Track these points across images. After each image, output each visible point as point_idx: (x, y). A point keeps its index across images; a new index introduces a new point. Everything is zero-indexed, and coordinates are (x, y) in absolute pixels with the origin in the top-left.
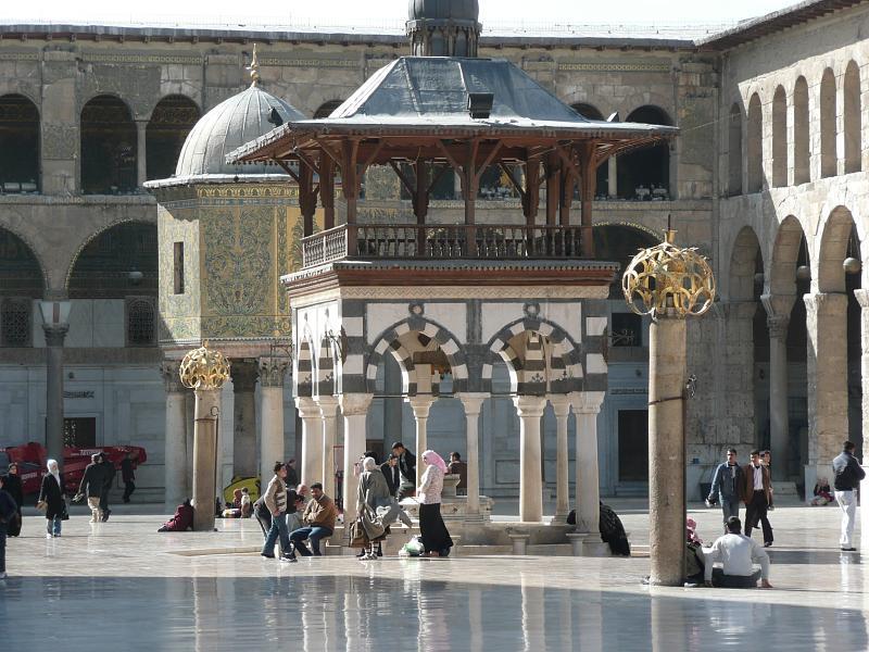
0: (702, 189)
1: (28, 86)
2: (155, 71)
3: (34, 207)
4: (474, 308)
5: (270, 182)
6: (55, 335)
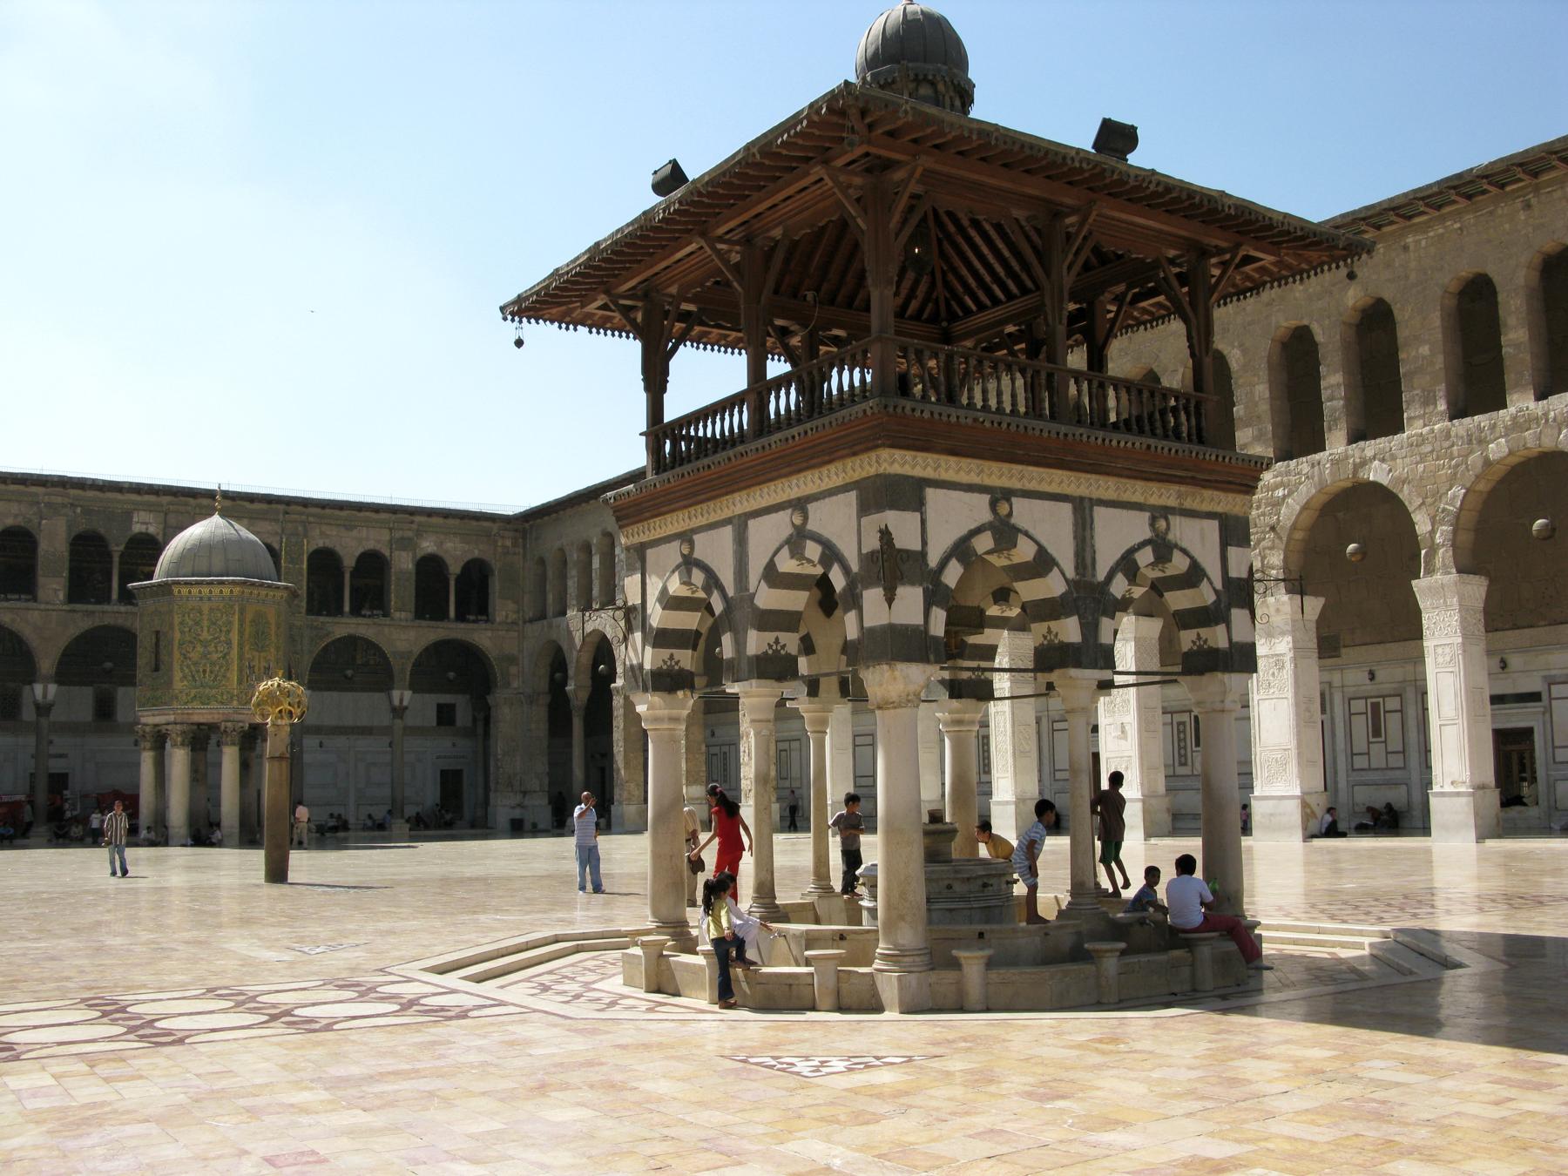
0: (512, 617)
2: (128, 516)
4: (1083, 510)
5: (233, 582)
6: (43, 709)
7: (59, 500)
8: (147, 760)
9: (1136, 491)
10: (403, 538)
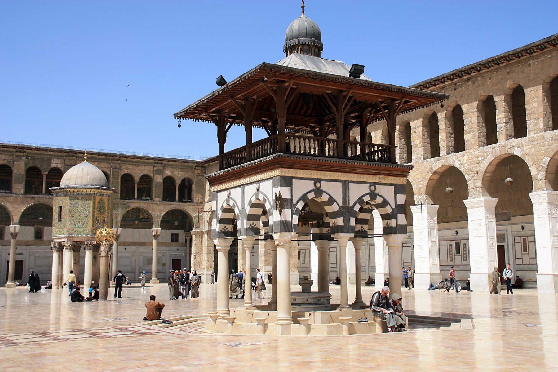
1: (9, 162)
2: (50, 160)
4: (346, 185)
6: (14, 235)
7: (21, 154)
8: (55, 255)
9: (364, 178)
10: (158, 170)
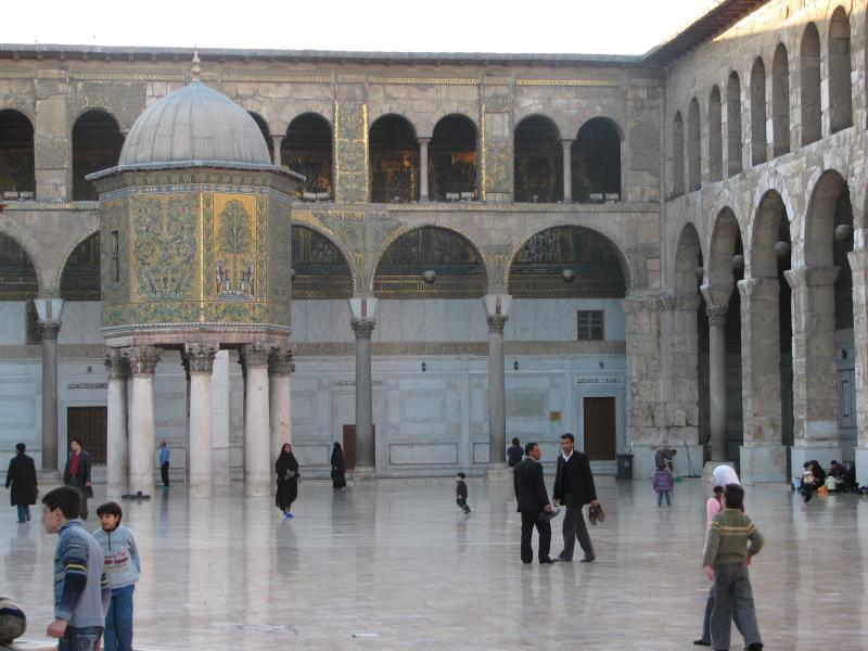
0: (651, 193)
3: (28, 213)
8: (114, 388)
